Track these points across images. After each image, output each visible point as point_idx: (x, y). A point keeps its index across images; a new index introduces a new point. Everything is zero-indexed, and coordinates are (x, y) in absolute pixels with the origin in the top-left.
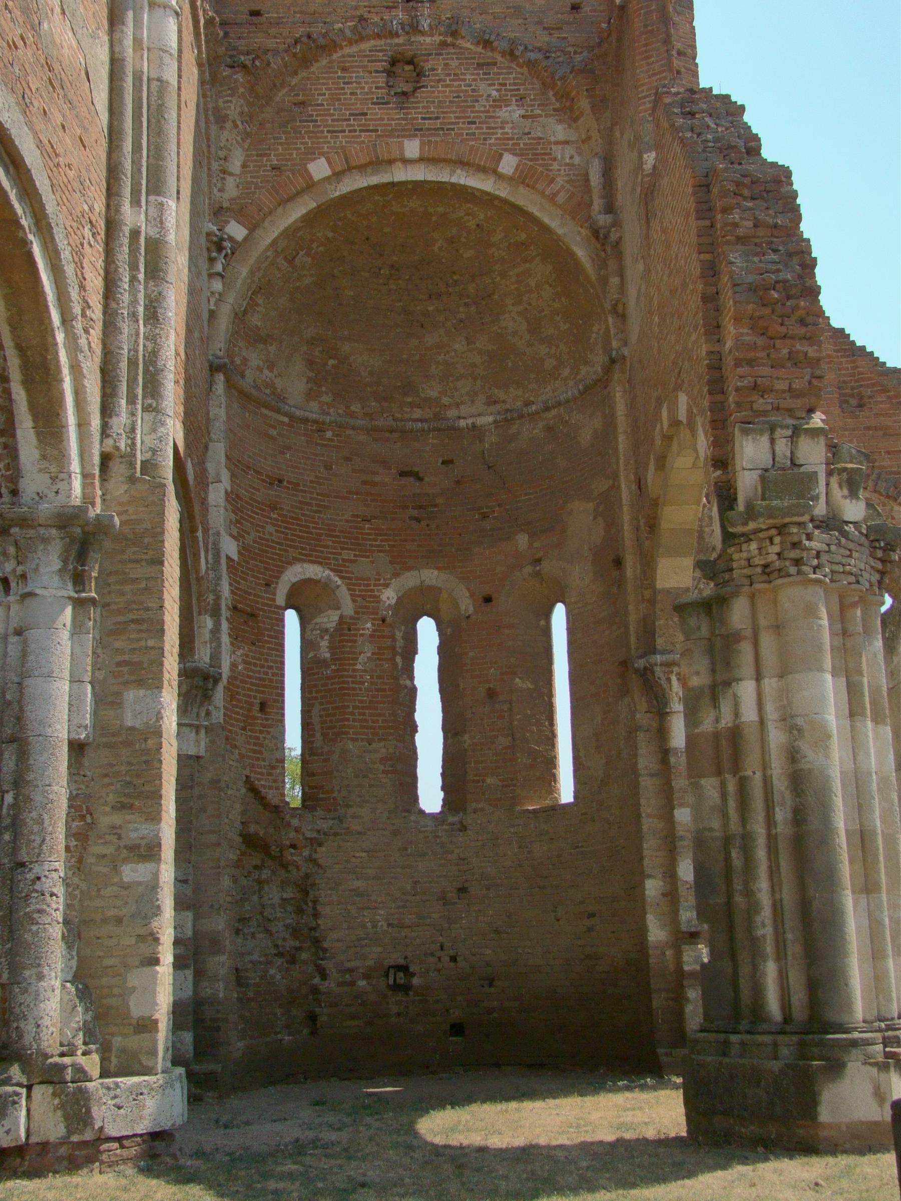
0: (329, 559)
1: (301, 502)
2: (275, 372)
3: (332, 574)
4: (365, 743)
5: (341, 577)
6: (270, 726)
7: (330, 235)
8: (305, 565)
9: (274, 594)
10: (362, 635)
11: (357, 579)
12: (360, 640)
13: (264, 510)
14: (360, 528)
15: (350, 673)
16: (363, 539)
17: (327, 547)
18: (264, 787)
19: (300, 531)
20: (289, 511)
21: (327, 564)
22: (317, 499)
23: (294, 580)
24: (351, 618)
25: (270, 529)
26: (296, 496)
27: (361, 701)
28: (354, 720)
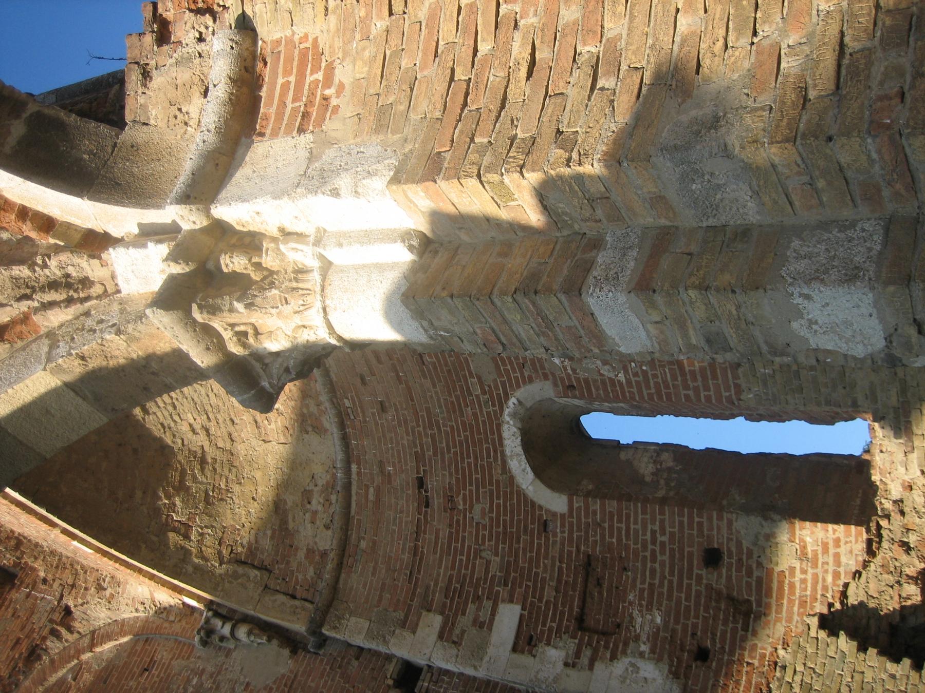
0: (488, 413)
1: (435, 454)
2: (311, 487)
3: (507, 411)
4: (740, 370)
5: (507, 398)
6: (739, 544)
7: (139, 494)
8: (508, 452)
9: (554, 514)
10: (574, 370)
11: (500, 375)
12: (582, 375)
13: (458, 521)
14: (435, 368)
15: (635, 390)
16: (446, 365)
17: (475, 414)
18: (836, 575)
19: (469, 457)
20: (451, 474)
21: (497, 419)
22: (424, 428)
23: (531, 475)
24: (555, 385)
25: (477, 508)
26: (430, 460)
27: (674, 378)
28: (707, 389)
